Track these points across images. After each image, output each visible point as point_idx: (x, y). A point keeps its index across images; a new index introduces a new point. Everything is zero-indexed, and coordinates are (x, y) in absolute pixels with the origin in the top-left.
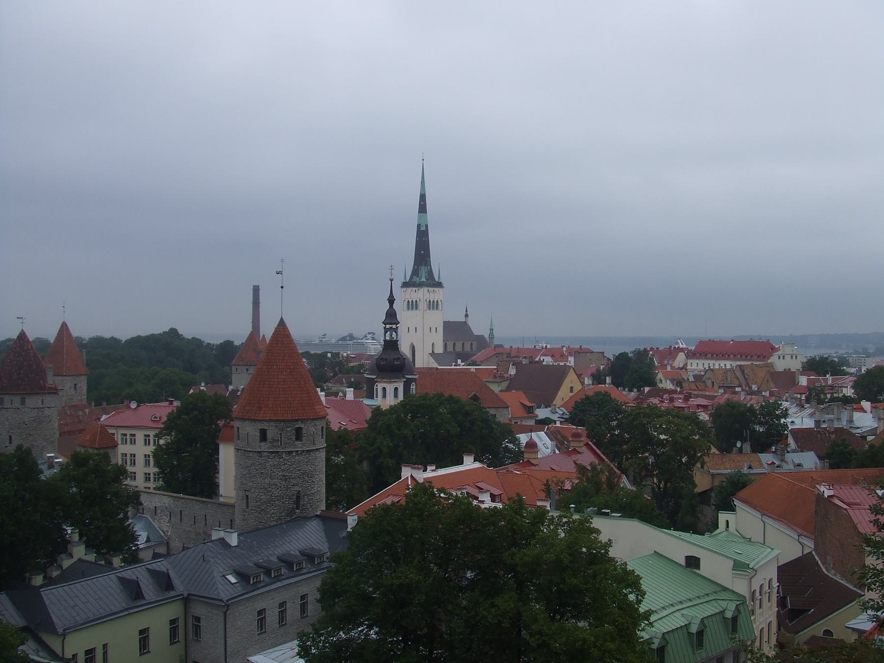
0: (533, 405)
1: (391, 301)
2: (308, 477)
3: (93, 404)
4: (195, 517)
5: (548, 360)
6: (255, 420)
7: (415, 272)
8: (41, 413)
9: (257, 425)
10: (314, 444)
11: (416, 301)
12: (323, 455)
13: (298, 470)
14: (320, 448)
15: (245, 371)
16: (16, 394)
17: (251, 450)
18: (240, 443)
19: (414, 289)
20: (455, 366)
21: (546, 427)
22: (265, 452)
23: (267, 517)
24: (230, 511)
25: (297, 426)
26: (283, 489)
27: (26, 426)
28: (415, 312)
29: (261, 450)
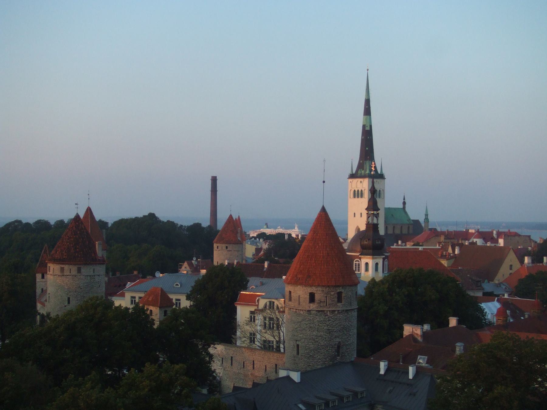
0: (480, 279)
1: (373, 191)
2: (346, 331)
3: (111, 273)
4: (244, 362)
5: (479, 242)
6: (306, 286)
7: (361, 166)
8: (93, 280)
9: (307, 290)
10: (351, 305)
11: (362, 191)
12: (355, 314)
13: (339, 325)
14: (355, 309)
15: (225, 249)
16: (74, 264)
17: (302, 309)
18: (292, 303)
19: (360, 180)
20: (396, 246)
21: (496, 299)
22: (314, 310)
23: (315, 362)
24: (275, 358)
25: (338, 291)
26: (327, 340)
27: (81, 290)
28: (360, 199)
29: (309, 309)
